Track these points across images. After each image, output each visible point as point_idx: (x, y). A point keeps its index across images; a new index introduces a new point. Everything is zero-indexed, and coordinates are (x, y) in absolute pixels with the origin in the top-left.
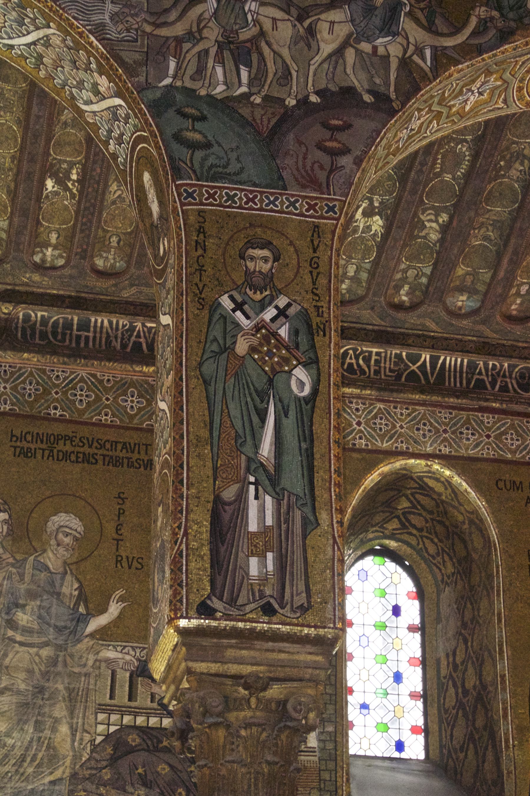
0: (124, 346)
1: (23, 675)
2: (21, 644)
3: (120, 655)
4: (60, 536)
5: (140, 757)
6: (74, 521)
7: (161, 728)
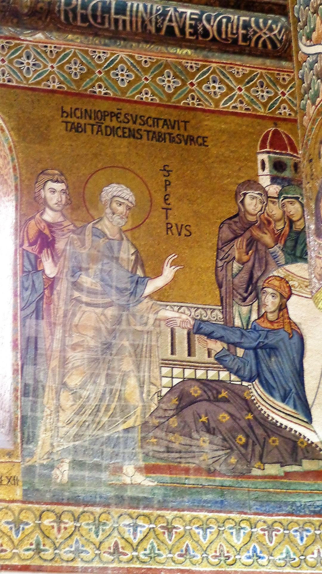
0: (158, 30)
1: (91, 333)
2: (88, 304)
3: (177, 315)
4: (114, 205)
5: (203, 406)
6: (125, 191)
7: (219, 381)
